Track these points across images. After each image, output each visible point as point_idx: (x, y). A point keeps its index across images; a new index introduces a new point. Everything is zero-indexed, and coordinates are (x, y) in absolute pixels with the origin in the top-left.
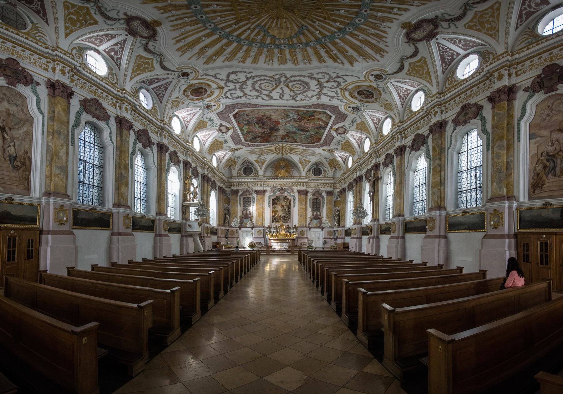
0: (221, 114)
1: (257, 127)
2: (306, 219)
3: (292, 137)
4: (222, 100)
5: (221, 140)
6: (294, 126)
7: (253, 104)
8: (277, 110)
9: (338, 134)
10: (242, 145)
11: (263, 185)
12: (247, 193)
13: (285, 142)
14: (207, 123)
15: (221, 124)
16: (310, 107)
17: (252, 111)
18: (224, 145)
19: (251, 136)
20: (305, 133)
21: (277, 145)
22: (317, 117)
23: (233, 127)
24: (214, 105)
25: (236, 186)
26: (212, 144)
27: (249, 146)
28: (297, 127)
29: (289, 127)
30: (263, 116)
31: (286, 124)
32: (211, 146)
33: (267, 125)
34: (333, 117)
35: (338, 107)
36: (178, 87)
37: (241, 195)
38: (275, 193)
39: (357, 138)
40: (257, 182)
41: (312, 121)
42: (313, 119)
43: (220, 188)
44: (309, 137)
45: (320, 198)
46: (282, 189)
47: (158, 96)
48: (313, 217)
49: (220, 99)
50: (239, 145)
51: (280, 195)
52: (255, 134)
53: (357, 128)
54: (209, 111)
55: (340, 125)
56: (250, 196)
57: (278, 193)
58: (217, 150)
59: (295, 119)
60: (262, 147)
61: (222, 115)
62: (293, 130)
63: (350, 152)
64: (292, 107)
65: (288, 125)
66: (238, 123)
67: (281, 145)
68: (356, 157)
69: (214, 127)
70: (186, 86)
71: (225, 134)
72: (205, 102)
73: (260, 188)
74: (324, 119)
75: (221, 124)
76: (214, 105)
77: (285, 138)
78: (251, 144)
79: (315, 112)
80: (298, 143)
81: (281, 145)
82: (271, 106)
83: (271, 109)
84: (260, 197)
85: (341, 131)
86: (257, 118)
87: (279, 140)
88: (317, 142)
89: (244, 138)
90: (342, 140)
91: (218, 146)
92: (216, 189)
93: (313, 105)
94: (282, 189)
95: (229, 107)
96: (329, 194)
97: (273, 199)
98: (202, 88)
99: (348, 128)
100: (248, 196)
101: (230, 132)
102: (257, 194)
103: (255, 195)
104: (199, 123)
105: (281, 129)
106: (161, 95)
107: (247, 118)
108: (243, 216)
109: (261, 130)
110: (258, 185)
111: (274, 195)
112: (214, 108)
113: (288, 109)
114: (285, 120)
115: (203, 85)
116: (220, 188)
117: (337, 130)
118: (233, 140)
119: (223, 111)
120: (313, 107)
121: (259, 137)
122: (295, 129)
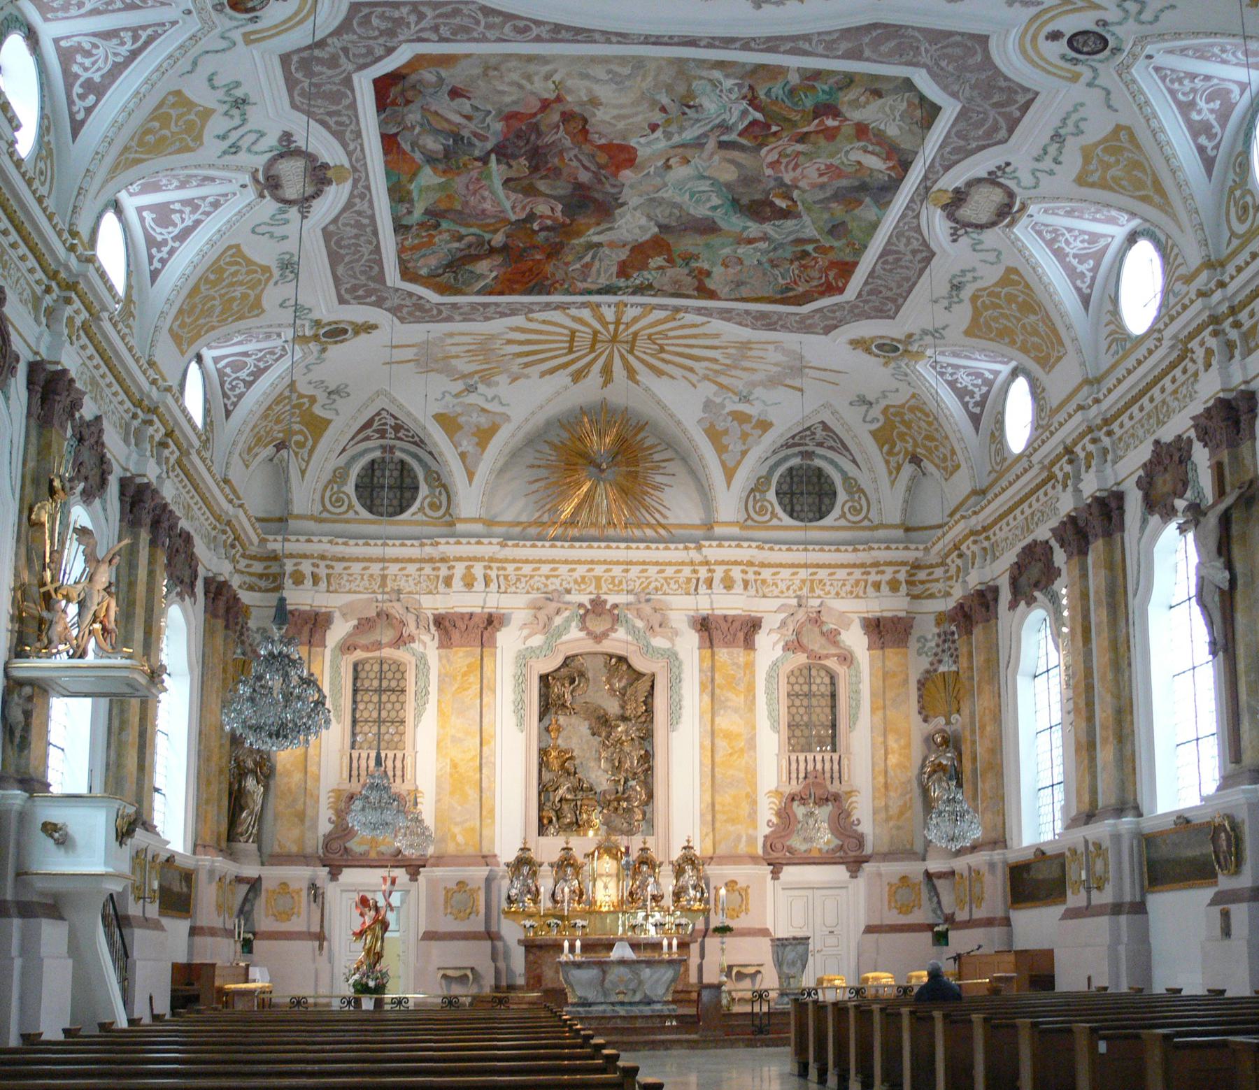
0: (305, 64)
1: (497, 184)
3: (688, 258)
5: (264, 253)
6: (714, 182)
7: (509, 17)
8: (639, 63)
9: (960, 227)
10: (379, 304)
11: (479, 585)
12: (387, 636)
13: (639, 290)
14: (207, 114)
15: (287, 137)
16: (830, 42)
17: (490, 67)
18: (272, 295)
19: (444, 246)
20: (768, 228)
21: (586, 314)
22: (857, 116)
23: (358, 170)
25: (308, 582)
26: (203, 279)
27: (419, 312)
28: (728, 186)
29: (680, 186)
30: (546, 105)
31: (667, 167)
32: (195, 290)
33: (556, 172)
34: (950, 110)
35: (983, 40)
37: (347, 647)
39: (1076, 246)
40: (443, 560)
41: (822, 142)
42: (831, 134)
43: (217, 592)
44: (788, 253)
48: (795, 787)
50: (360, 300)
52: (471, 232)
53: (1081, 181)
54: (237, 35)
55: (978, 166)
56: (400, 654)
58: (223, 322)
59: (724, 127)
60: (498, 325)
61: (310, 74)
62: (701, 211)
63: (1024, 350)
64: (727, 42)
65: (680, 172)
66: (389, 142)
67: (609, 314)
68: (1063, 379)
69: (243, 158)
71: (293, 212)
74: (892, 131)
75: (287, 137)
77: (644, 266)
78: (432, 297)
79: (849, 80)
80: (712, 295)
81: (609, 314)
82: (608, 37)
83: (605, 60)
84: (462, 657)
85: (982, 205)
86: (510, 117)
87: (603, 281)
88: (830, 289)
89: (401, 250)
90: (983, 270)
91: (238, 291)
92: (193, 594)
93: (847, 33)
99: (1027, 179)
100: (387, 652)
101: (334, 199)
103: (427, 644)
104: (159, 115)
105: (634, 201)
107: (451, 111)
109: (510, 205)
110: (448, 581)
111: (550, 647)
113: (701, 63)
114: (668, 136)
116: (217, 592)
117: (959, 197)
118: (334, 259)
119: (321, 44)
120: (844, 46)
121: (492, 251)
122: (716, 201)
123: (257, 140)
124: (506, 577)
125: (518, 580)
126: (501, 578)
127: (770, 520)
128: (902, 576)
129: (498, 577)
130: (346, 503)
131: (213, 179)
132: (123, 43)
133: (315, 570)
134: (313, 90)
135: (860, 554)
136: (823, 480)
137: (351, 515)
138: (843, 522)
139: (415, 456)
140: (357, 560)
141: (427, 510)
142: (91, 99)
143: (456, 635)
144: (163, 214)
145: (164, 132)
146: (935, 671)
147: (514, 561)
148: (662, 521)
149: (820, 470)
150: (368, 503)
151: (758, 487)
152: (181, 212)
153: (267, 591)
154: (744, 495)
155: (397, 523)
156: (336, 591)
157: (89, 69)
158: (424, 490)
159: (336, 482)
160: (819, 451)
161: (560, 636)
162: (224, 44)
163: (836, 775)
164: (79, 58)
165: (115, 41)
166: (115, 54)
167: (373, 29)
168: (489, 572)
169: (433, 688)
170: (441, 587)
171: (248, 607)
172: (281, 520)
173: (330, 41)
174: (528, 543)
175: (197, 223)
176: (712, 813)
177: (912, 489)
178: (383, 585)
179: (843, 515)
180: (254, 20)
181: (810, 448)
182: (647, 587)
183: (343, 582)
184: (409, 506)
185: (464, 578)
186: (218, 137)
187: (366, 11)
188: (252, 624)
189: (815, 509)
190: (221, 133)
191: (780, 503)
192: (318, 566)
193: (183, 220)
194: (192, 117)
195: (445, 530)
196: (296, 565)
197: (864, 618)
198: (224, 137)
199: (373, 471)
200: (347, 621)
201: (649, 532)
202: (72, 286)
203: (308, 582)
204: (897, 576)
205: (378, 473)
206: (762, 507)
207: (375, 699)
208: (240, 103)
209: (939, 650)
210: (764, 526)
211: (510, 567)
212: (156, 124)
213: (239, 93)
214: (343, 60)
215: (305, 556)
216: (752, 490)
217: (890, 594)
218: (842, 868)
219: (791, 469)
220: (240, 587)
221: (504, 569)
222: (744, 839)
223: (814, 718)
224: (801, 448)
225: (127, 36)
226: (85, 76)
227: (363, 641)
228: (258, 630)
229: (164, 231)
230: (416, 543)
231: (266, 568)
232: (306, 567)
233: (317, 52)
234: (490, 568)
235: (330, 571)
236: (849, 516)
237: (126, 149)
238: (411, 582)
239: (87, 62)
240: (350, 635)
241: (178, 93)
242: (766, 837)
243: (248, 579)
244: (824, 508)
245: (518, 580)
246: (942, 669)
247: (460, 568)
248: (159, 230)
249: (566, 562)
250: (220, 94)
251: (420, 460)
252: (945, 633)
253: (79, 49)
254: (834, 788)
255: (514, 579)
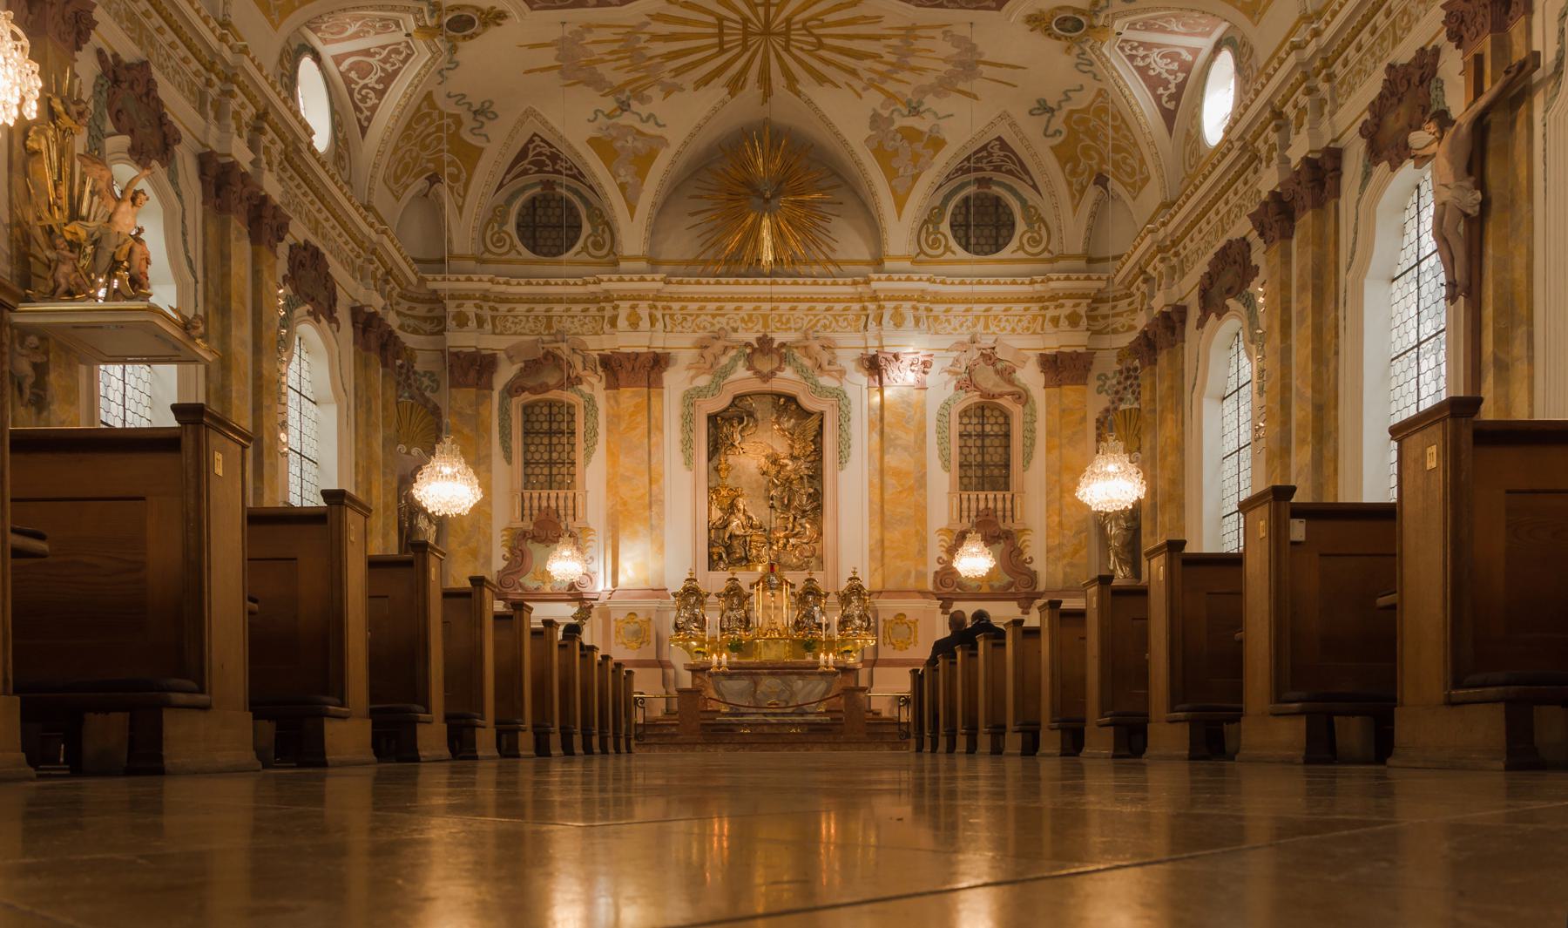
2: (923, 540)
11: (645, 324)
37: (512, 390)
38: (725, 372)
40: (608, 299)
45: (1005, 402)
46: (764, 346)
51: (757, 385)
56: (568, 396)
57: (741, 372)
73: (628, 341)
84: (629, 397)
94: (764, 346)
96: (1059, 368)
97: (712, 419)
100: (553, 395)
102: (613, 384)
103: (595, 386)
108: (528, 525)
110: (613, 322)
124: (672, 316)
125: (685, 319)
126: (667, 318)
127: (944, 253)
128: (1082, 310)
129: (663, 316)
130: (508, 241)
133: (479, 311)
135: (1038, 287)
136: (1001, 210)
137: (513, 255)
138: (1021, 254)
139: (576, 192)
140: (521, 300)
141: (591, 249)
143: (622, 376)
146: (1116, 409)
147: (679, 300)
148: (832, 256)
149: (997, 201)
150: (531, 242)
151: (931, 219)
153: (432, 334)
154: (916, 226)
155: (560, 263)
156: (501, 334)
158: (586, 228)
159: (497, 221)
160: (997, 176)
161: (724, 378)
163: (1008, 514)
168: (654, 311)
169: (602, 430)
170: (607, 327)
171: (413, 349)
172: (442, 261)
174: (693, 280)
176: (880, 550)
177: (1097, 215)
178: (549, 326)
179: (1021, 247)
181: (987, 174)
182: (815, 325)
183: (508, 324)
184: (572, 245)
185: (628, 319)
188: (418, 367)
189: (992, 241)
191: (955, 237)
192: (481, 308)
195: (608, 269)
196: (458, 306)
197: (1041, 354)
199: (535, 209)
200: (513, 363)
201: (816, 269)
203: (473, 324)
204: (1077, 309)
205: (540, 212)
206: (936, 240)
207: (546, 441)
209: (1120, 387)
210: (935, 260)
211: (676, 306)
215: (467, 297)
216: (926, 222)
217: (1069, 328)
218: (1014, 604)
219: (966, 200)
220: (401, 327)
221: (670, 308)
222: (913, 573)
223: (987, 458)
224: (980, 174)
227: (530, 383)
228: (426, 372)
230: (579, 281)
231: (430, 310)
232: (469, 308)
234: (656, 307)
235: (495, 313)
236: (1027, 248)
238: (577, 324)
240: (517, 377)
242: (936, 572)
243: (411, 322)
244: (1001, 241)
245: (685, 319)
246: (1123, 407)
247: (625, 306)
249: (732, 300)
251: (581, 197)
252: (1128, 370)
254: (1007, 525)
255: (680, 317)
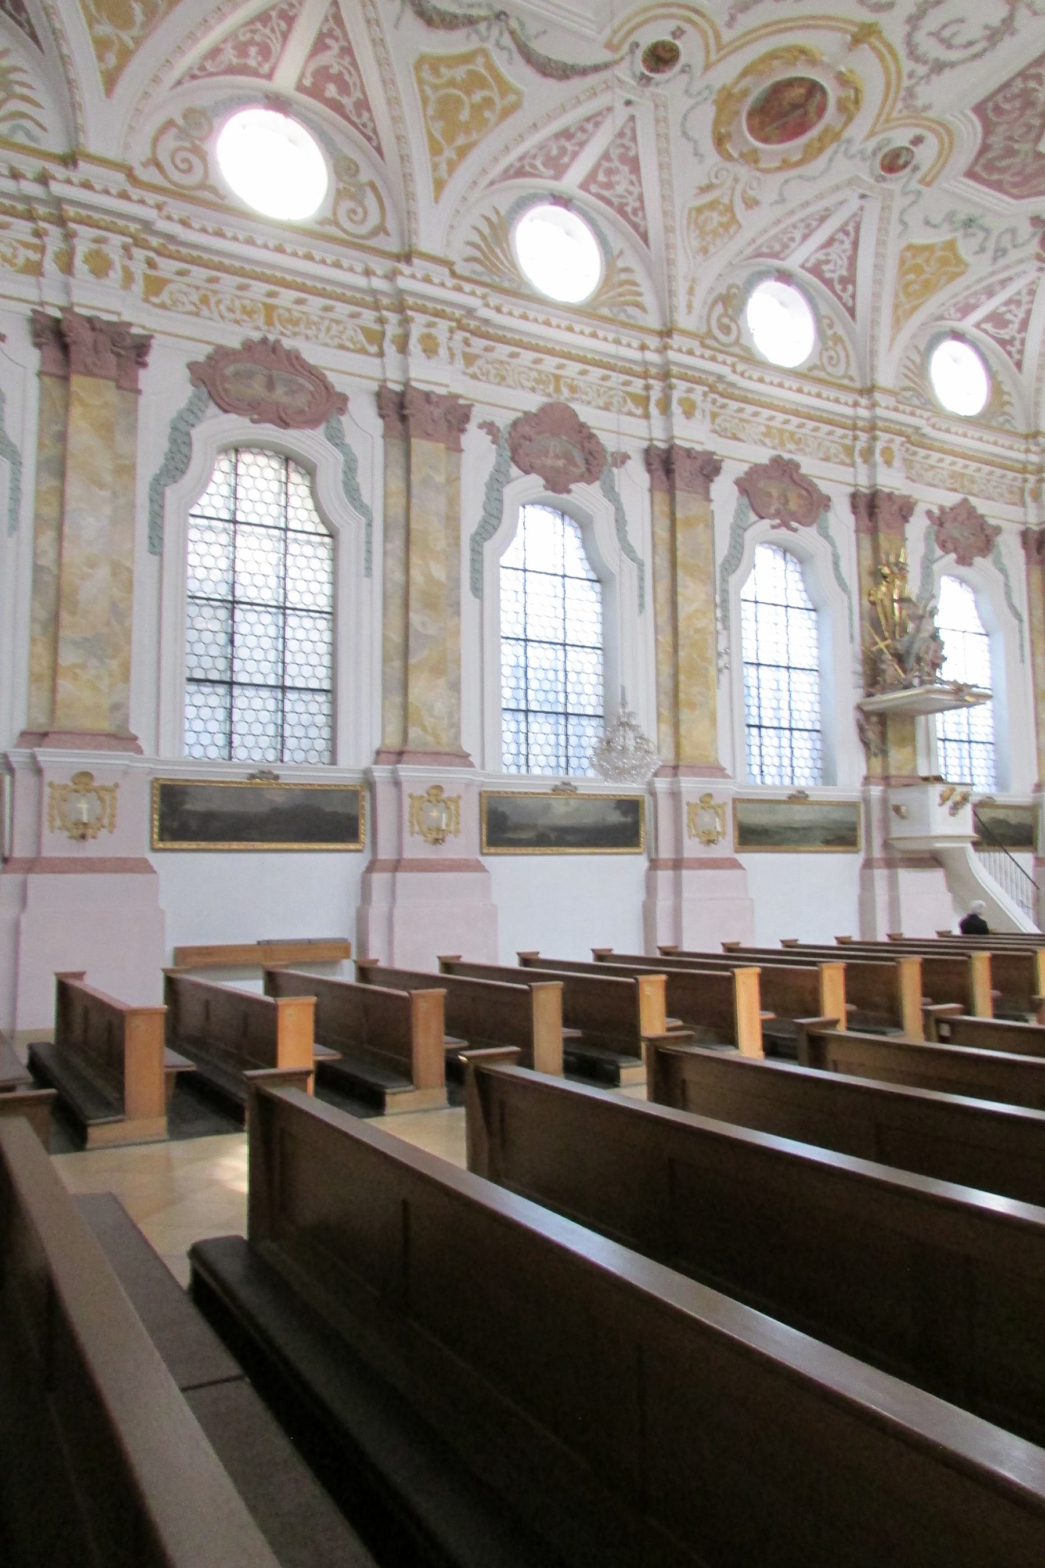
0: (990, 167)
4: (925, 94)
14: (950, 246)
24: (918, 140)
36: (675, 133)
47: (621, 210)
49: (911, 94)
61: (1002, 170)
69: (1013, 255)
70: (708, 113)
72: (855, 148)
76: (918, 140)
95: (998, 110)
98: (790, 83)
106: (632, 203)
112: (926, 155)
115: (775, 63)
119: (985, 148)
123: (1014, 239)
131: (1010, 279)
132: (842, 242)
134: (1016, 179)
142: (850, 287)
144: (997, 319)
145: (925, 276)
152: (1010, 311)
157: (836, 270)
162: (911, 198)
164: (825, 268)
165: (836, 244)
166: (844, 251)
167: (1009, 112)
173: (989, 142)
175: (1029, 312)
180: (916, 169)
186: (976, 253)
187: (990, 105)
190: (977, 248)
193: (1015, 316)
194: (939, 254)
198: (982, 250)
202: (872, 428)
208: (969, 223)
212: (912, 276)
213: (962, 216)
214: (1016, 146)
225: (841, 236)
226: (835, 276)
229: (1007, 330)
233: (990, 155)
237: (896, 307)
239: (831, 267)
241: (910, 247)
248: (1002, 332)
250: (946, 227)
253: (819, 263)
